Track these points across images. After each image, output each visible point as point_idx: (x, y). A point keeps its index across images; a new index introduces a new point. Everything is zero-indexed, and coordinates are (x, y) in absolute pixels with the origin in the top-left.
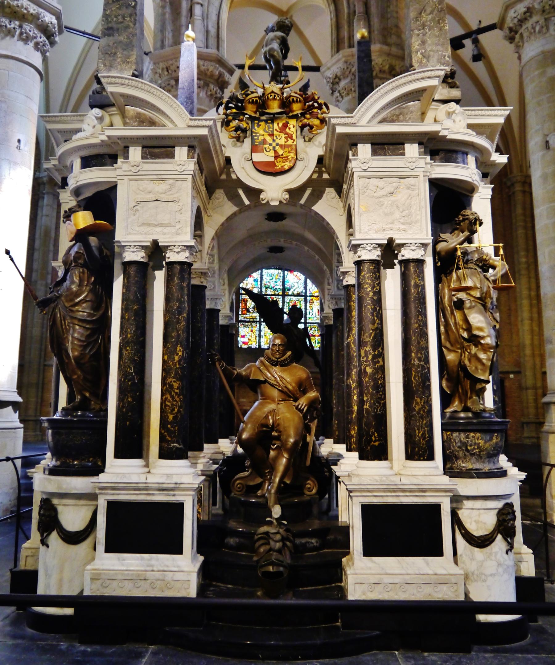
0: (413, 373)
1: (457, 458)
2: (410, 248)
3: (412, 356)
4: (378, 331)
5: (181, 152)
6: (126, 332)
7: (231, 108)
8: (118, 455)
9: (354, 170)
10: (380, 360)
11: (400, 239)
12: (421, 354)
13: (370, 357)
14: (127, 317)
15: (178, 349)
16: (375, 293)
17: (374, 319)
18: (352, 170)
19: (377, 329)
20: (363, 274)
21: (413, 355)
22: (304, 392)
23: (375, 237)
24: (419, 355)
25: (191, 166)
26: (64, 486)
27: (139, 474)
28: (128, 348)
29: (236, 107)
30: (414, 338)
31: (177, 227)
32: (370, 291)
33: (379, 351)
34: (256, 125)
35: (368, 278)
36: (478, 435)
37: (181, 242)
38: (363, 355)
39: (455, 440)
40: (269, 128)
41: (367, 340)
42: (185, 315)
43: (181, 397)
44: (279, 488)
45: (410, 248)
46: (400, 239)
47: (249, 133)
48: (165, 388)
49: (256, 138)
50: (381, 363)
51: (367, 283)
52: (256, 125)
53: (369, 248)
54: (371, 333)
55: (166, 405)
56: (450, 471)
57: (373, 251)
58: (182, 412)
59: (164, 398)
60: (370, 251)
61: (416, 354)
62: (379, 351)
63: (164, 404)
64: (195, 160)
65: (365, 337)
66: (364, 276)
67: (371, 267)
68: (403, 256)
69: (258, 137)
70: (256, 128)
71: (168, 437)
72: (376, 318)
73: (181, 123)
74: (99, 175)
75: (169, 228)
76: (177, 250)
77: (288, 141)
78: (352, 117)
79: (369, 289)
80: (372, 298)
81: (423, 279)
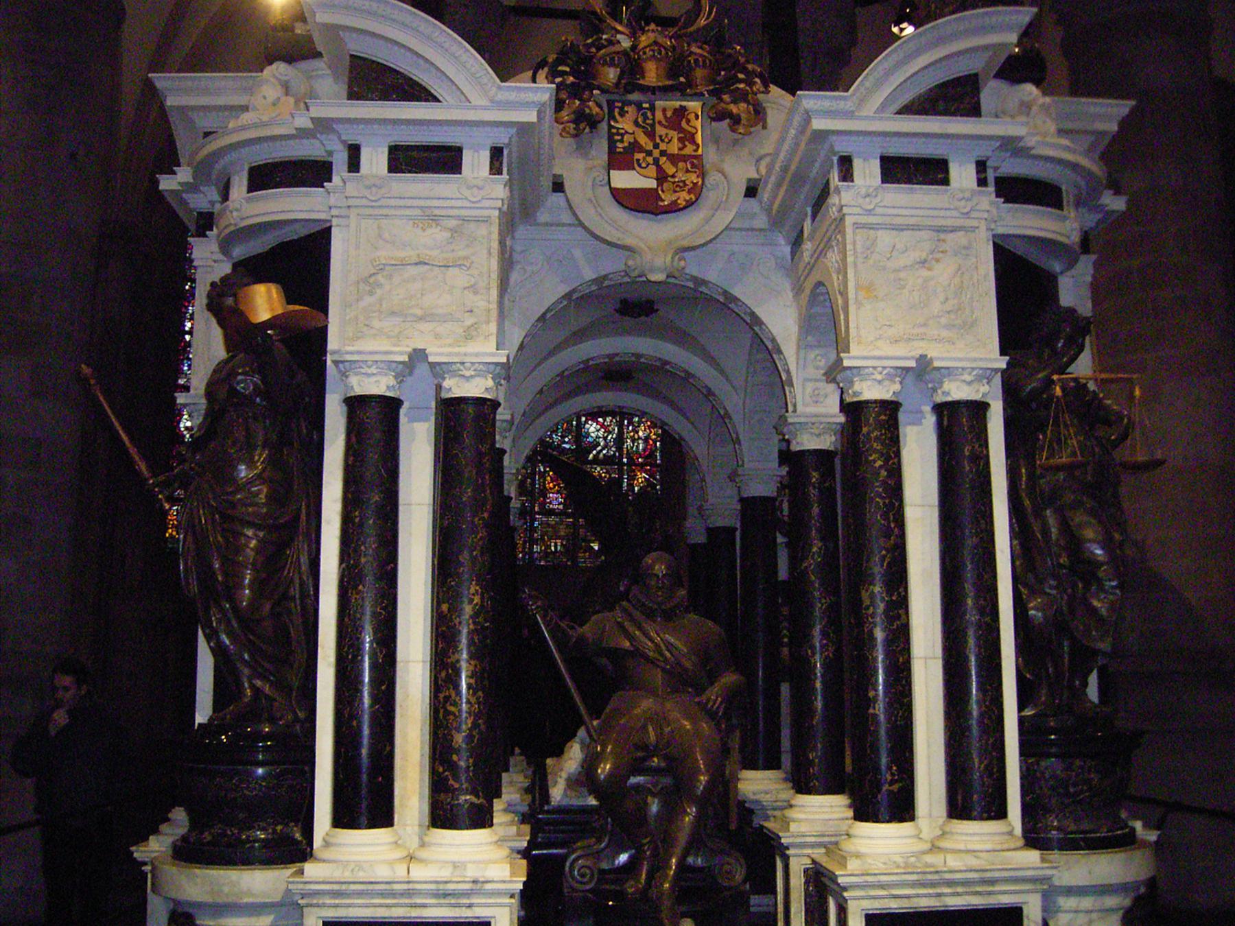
1: (1048, 811)
2: (963, 378)
3: (966, 604)
5: (476, 163)
6: (355, 551)
8: (344, 818)
9: (845, 210)
11: (943, 359)
12: (985, 600)
13: (882, 606)
14: (357, 520)
15: (472, 590)
18: (840, 210)
20: (865, 430)
21: (969, 601)
23: (890, 354)
24: (982, 602)
25: (498, 190)
26: (226, 889)
27: (391, 863)
28: (361, 587)
31: (468, 323)
32: (881, 467)
33: (899, 594)
34: (617, 110)
35: (877, 439)
36: (1089, 763)
37: (477, 355)
39: (1043, 773)
40: (646, 118)
42: (486, 515)
43: (480, 693)
45: (963, 378)
46: (943, 359)
48: (443, 674)
49: (617, 137)
51: (875, 451)
52: (617, 110)
53: (879, 377)
54: (884, 556)
56: (1033, 839)
57: (886, 383)
58: (483, 727)
59: (441, 696)
60: (879, 382)
61: (977, 598)
62: (899, 594)
63: (442, 711)
64: (505, 176)
67: (883, 417)
68: (947, 394)
69: (622, 135)
70: (618, 117)
71: (451, 782)
73: (477, 99)
74: (294, 206)
75: (449, 325)
76: (468, 373)
77: (685, 146)
78: (845, 98)
79: (879, 463)
80: (884, 483)
81: (986, 444)
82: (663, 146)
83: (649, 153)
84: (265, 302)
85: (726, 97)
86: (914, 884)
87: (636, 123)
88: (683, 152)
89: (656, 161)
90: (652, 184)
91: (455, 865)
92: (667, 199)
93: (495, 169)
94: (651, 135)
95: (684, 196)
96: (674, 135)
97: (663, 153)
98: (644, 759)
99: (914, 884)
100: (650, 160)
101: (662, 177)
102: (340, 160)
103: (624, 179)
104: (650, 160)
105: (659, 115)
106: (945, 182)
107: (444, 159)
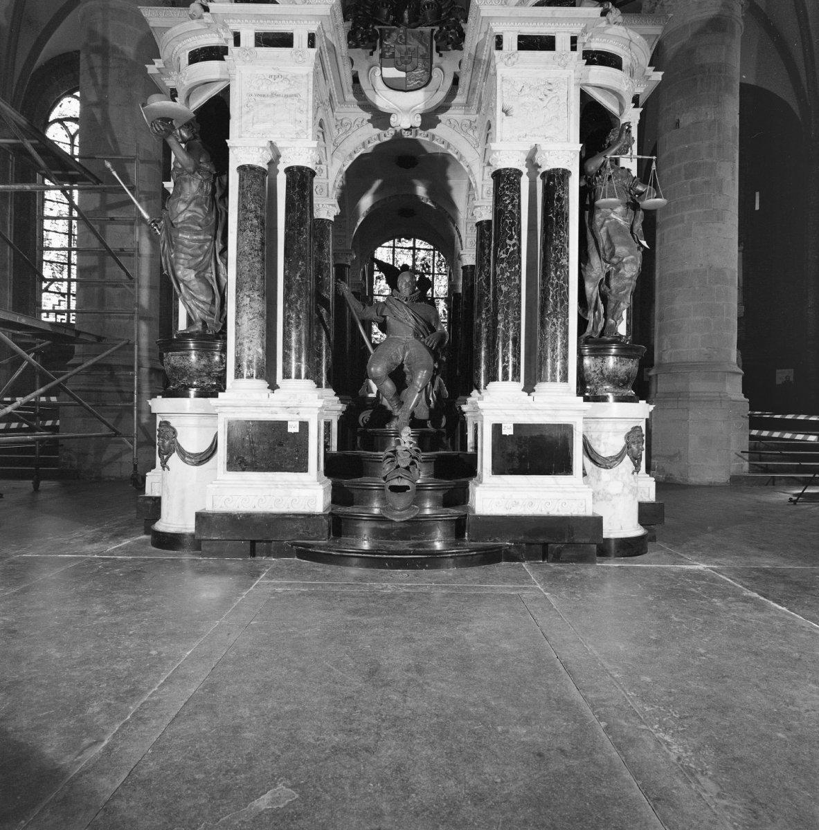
0: (551, 293)
4: (516, 248)
10: (517, 278)
12: (561, 272)
16: (514, 206)
17: (512, 234)
19: (514, 245)
20: (502, 185)
30: (554, 255)
32: (509, 203)
35: (507, 189)
38: (498, 272)
41: (504, 256)
50: (517, 282)
51: (507, 195)
65: (501, 253)
66: (503, 188)
72: (514, 233)
79: (508, 201)
80: (510, 211)
102: (231, 44)
107: (284, 40)
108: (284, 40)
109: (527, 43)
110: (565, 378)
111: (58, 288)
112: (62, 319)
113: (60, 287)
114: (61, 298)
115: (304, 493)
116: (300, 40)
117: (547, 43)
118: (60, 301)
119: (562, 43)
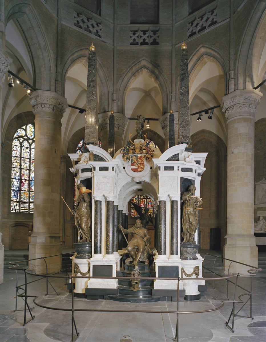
7: (125, 151)
22: (145, 236)
29: (127, 151)
40: (136, 158)
44: (138, 262)
47: (130, 159)
55: (107, 240)
74: (88, 175)
82: (139, 162)
83: (137, 163)
84: (84, 189)
85: (148, 154)
86: (164, 262)
87: (135, 158)
88: (142, 163)
89: (138, 165)
90: (137, 168)
91: (108, 259)
92: (139, 170)
93: (113, 170)
94: (137, 160)
95: (141, 170)
96: (140, 160)
97: (139, 163)
98: (135, 247)
99: (164, 262)
100: (137, 164)
101: (138, 167)
103: (133, 167)
104: (137, 164)
105: (138, 158)
106: (173, 170)
107: (106, 169)
108: (106, 169)
109: (166, 168)
110: (177, 254)
111: (16, 200)
112: (17, 211)
113: (17, 199)
114: (17, 203)
115: (112, 284)
116: (110, 169)
117: (171, 168)
118: (17, 204)
119: (176, 168)
